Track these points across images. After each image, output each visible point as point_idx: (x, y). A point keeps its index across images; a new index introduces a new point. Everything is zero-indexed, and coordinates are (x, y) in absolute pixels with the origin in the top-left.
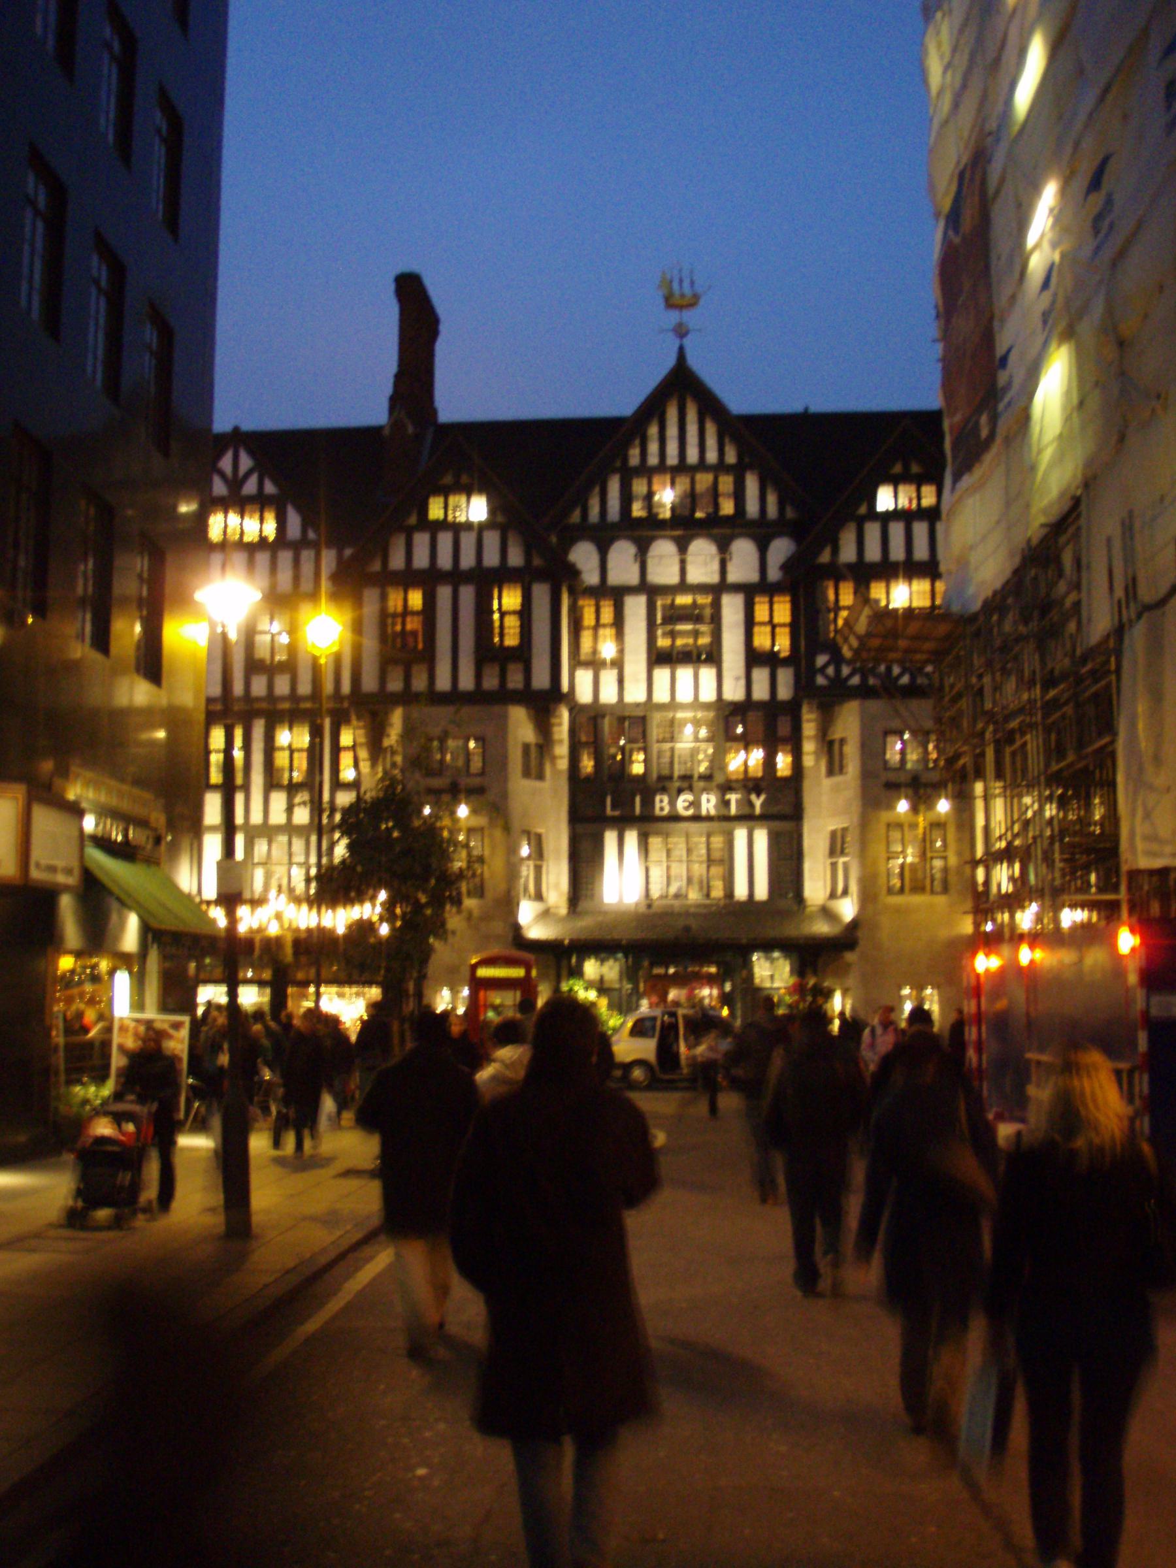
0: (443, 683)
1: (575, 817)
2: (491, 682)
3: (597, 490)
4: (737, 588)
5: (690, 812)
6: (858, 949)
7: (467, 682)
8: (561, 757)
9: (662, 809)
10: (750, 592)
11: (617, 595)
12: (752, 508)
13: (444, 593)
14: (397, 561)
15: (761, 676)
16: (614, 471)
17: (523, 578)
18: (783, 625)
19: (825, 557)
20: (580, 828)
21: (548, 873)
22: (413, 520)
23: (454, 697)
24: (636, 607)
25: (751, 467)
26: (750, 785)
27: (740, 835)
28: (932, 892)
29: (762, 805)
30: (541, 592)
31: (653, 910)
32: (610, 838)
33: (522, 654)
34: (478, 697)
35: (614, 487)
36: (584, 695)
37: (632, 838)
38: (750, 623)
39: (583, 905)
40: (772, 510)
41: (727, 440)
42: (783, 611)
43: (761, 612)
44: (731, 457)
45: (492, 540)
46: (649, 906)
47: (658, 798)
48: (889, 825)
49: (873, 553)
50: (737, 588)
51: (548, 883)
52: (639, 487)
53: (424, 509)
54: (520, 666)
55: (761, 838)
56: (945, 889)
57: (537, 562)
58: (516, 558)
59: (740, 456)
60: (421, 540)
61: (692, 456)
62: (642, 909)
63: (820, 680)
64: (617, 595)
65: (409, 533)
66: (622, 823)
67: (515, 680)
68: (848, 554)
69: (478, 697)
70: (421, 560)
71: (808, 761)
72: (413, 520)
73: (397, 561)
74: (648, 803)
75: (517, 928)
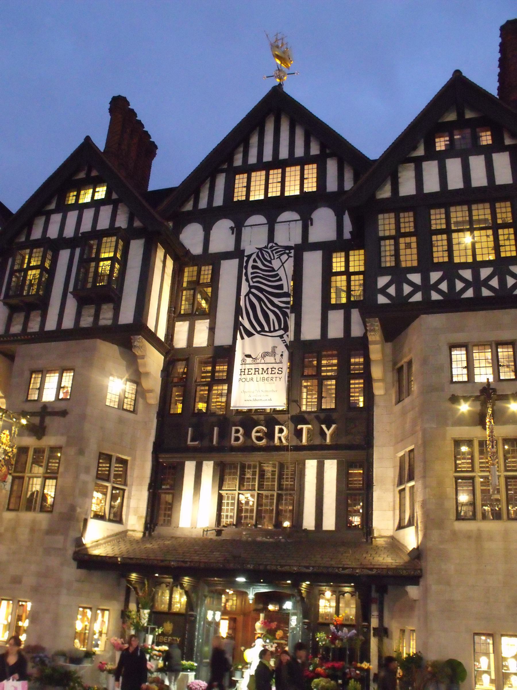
0: (51, 325)
1: (159, 448)
2: (87, 321)
5: (263, 442)
7: (68, 323)
9: (237, 439)
10: (328, 249)
11: (215, 260)
12: (332, 186)
13: (64, 255)
14: (37, 234)
15: (336, 319)
16: (222, 171)
17: (126, 237)
19: (385, 193)
20: (165, 459)
21: (129, 498)
22: (53, 206)
23: (60, 335)
24: (229, 269)
25: (331, 156)
26: (324, 417)
29: (332, 436)
30: (137, 247)
31: (224, 537)
32: (190, 467)
33: (111, 294)
34: (78, 333)
35: (221, 181)
36: (180, 341)
37: (208, 468)
38: (328, 273)
39: (161, 530)
41: (312, 139)
43: (338, 263)
44: (315, 150)
45: (106, 212)
46: (219, 533)
47: (234, 428)
49: (431, 185)
51: (128, 506)
52: (241, 180)
53: (63, 197)
54: (111, 306)
55: (331, 467)
57: (137, 224)
58: (122, 222)
60: (56, 218)
61: (284, 154)
62: (212, 535)
63: (382, 300)
65: (48, 214)
66: (200, 454)
67: (106, 318)
69: (78, 333)
70: (53, 233)
72: (53, 206)
73: (37, 234)
74: (224, 434)
75: (79, 542)
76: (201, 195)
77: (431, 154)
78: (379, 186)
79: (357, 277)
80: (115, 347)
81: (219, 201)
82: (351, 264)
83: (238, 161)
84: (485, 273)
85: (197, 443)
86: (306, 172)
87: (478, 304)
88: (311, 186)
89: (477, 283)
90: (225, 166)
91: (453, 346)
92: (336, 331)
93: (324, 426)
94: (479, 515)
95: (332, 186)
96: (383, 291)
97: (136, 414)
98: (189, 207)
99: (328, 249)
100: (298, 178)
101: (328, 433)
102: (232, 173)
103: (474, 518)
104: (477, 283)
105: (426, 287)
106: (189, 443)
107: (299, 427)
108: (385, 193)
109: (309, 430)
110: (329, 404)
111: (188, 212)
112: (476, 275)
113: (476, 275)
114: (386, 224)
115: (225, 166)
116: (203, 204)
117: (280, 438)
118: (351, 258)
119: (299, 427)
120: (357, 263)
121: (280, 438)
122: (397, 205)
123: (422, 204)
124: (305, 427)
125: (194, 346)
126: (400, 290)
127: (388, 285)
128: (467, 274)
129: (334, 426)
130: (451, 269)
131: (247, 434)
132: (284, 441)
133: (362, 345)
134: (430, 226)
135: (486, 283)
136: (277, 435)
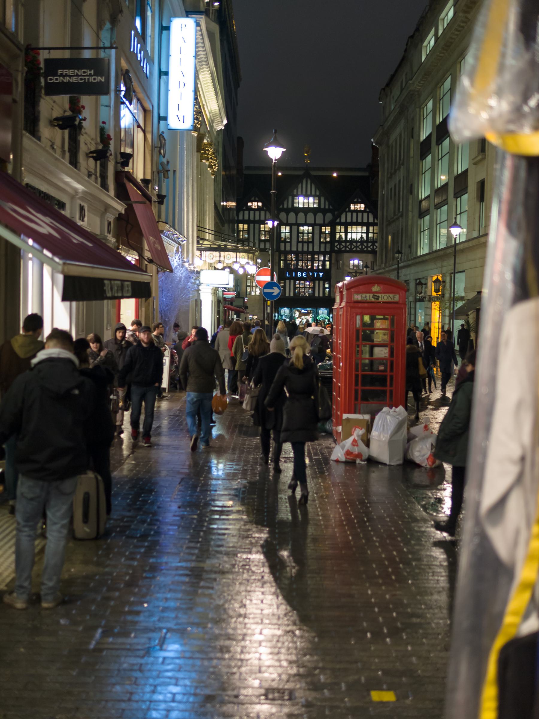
12: (322, 207)
13: (252, 225)
15: (323, 246)
27: (317, 282)
40: (327, 207)
44: (318, 193)
49: (349, 220)
61: (309, 193)
63: (336, 249)
68: (343, 220)
81: (290, 206)
89: (357, 247)
95: (322, 207)
98: (281, 207)
104: (357, 247)
108: (338, 221)
110: (320, 268)
112: (357, 244)
116: (285, 206)
122: (341, 224)
126: (340, 246)
131: (302, 274)
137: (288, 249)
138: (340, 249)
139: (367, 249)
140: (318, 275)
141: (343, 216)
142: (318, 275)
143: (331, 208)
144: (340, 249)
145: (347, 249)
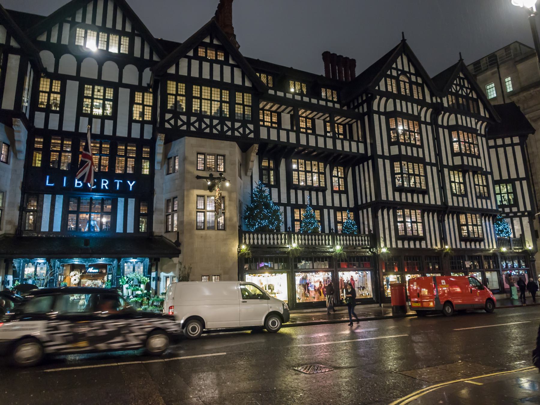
3: (57, 25)
4: (126, 86)
6: (180, 256)
8: (20, 152)
10: (133, 89)
15: (136, 128)
16: (68, 22)
18: (149, 106)
19: (172, 70)
25: (138, 35)
27: (121, 202)
28: (218, 229)
29: (132, 186)
35: (66, 28)
40: (147, 56)
42: (149, 99)
43: (138, 97)
44: (128, 29)
48: (198, 196)
50: (126, 86)
56: (224, 229)
59: (133, 29)
61: (109, 25)
63: (167, 125)
64: (64, 79)
68: (183, 72)
71: (157, 167)
76: (53, 33)
77: (196, 56)
78: (170, 66)
79: (148, 108)
80: (4, 125)
82: (145, 100)
83: (79, 19)
84: (215, 122)
85: (52, 185)
86: (122, 40)
87: (211, 136)
88: (124, 50)
89: (211, 126)
90: (70, 19)
91: (198, 153)
92: (136, 133)
93: (129, 182)
94: (206, 228)
96: (168, 121)
97: (9, 164)
99: (133, 89)
100: (117, 42)
101: (131, 185)
102: (74, 25)
103: (204, 229)
104: (211, 126)
105: (189, 124)
106: (47, 184)
107: (116, 181)
108: (172, 70)
109: (120, 182)
110: (130, 171)
111: (42, 42)
112: (211, 122)
113: (211, 122)
114: (171, 87)
115: (70, 19)
116: (54, 39)
117: (104, 186)
118: (145, 97)
119: (116, 181)
120: (148, 100)
121: (104, 186)
122: (177, 78)
123: (190, 82)
124: (118, 181)
125: (49, 128)
126: (176, 122)
127: (170, 119)
128: (207, 121)
129: (134, 182)
130: (201, 116)
132: (107, 188)
133: (152, 144)
134: (192, 94)
135: (215, 127)
136: (103, 184)
137: (54, 125)
138: (176, 127)
139: (233, 133)
140: (124, 186)
141: (183, 63)
142: (124, 186)
143: (155, 58)
144: (176, 127)
145: (192, 129)
